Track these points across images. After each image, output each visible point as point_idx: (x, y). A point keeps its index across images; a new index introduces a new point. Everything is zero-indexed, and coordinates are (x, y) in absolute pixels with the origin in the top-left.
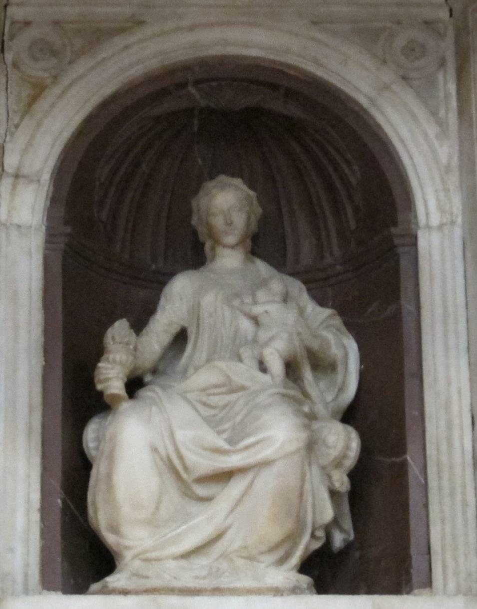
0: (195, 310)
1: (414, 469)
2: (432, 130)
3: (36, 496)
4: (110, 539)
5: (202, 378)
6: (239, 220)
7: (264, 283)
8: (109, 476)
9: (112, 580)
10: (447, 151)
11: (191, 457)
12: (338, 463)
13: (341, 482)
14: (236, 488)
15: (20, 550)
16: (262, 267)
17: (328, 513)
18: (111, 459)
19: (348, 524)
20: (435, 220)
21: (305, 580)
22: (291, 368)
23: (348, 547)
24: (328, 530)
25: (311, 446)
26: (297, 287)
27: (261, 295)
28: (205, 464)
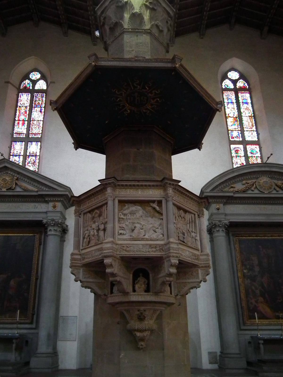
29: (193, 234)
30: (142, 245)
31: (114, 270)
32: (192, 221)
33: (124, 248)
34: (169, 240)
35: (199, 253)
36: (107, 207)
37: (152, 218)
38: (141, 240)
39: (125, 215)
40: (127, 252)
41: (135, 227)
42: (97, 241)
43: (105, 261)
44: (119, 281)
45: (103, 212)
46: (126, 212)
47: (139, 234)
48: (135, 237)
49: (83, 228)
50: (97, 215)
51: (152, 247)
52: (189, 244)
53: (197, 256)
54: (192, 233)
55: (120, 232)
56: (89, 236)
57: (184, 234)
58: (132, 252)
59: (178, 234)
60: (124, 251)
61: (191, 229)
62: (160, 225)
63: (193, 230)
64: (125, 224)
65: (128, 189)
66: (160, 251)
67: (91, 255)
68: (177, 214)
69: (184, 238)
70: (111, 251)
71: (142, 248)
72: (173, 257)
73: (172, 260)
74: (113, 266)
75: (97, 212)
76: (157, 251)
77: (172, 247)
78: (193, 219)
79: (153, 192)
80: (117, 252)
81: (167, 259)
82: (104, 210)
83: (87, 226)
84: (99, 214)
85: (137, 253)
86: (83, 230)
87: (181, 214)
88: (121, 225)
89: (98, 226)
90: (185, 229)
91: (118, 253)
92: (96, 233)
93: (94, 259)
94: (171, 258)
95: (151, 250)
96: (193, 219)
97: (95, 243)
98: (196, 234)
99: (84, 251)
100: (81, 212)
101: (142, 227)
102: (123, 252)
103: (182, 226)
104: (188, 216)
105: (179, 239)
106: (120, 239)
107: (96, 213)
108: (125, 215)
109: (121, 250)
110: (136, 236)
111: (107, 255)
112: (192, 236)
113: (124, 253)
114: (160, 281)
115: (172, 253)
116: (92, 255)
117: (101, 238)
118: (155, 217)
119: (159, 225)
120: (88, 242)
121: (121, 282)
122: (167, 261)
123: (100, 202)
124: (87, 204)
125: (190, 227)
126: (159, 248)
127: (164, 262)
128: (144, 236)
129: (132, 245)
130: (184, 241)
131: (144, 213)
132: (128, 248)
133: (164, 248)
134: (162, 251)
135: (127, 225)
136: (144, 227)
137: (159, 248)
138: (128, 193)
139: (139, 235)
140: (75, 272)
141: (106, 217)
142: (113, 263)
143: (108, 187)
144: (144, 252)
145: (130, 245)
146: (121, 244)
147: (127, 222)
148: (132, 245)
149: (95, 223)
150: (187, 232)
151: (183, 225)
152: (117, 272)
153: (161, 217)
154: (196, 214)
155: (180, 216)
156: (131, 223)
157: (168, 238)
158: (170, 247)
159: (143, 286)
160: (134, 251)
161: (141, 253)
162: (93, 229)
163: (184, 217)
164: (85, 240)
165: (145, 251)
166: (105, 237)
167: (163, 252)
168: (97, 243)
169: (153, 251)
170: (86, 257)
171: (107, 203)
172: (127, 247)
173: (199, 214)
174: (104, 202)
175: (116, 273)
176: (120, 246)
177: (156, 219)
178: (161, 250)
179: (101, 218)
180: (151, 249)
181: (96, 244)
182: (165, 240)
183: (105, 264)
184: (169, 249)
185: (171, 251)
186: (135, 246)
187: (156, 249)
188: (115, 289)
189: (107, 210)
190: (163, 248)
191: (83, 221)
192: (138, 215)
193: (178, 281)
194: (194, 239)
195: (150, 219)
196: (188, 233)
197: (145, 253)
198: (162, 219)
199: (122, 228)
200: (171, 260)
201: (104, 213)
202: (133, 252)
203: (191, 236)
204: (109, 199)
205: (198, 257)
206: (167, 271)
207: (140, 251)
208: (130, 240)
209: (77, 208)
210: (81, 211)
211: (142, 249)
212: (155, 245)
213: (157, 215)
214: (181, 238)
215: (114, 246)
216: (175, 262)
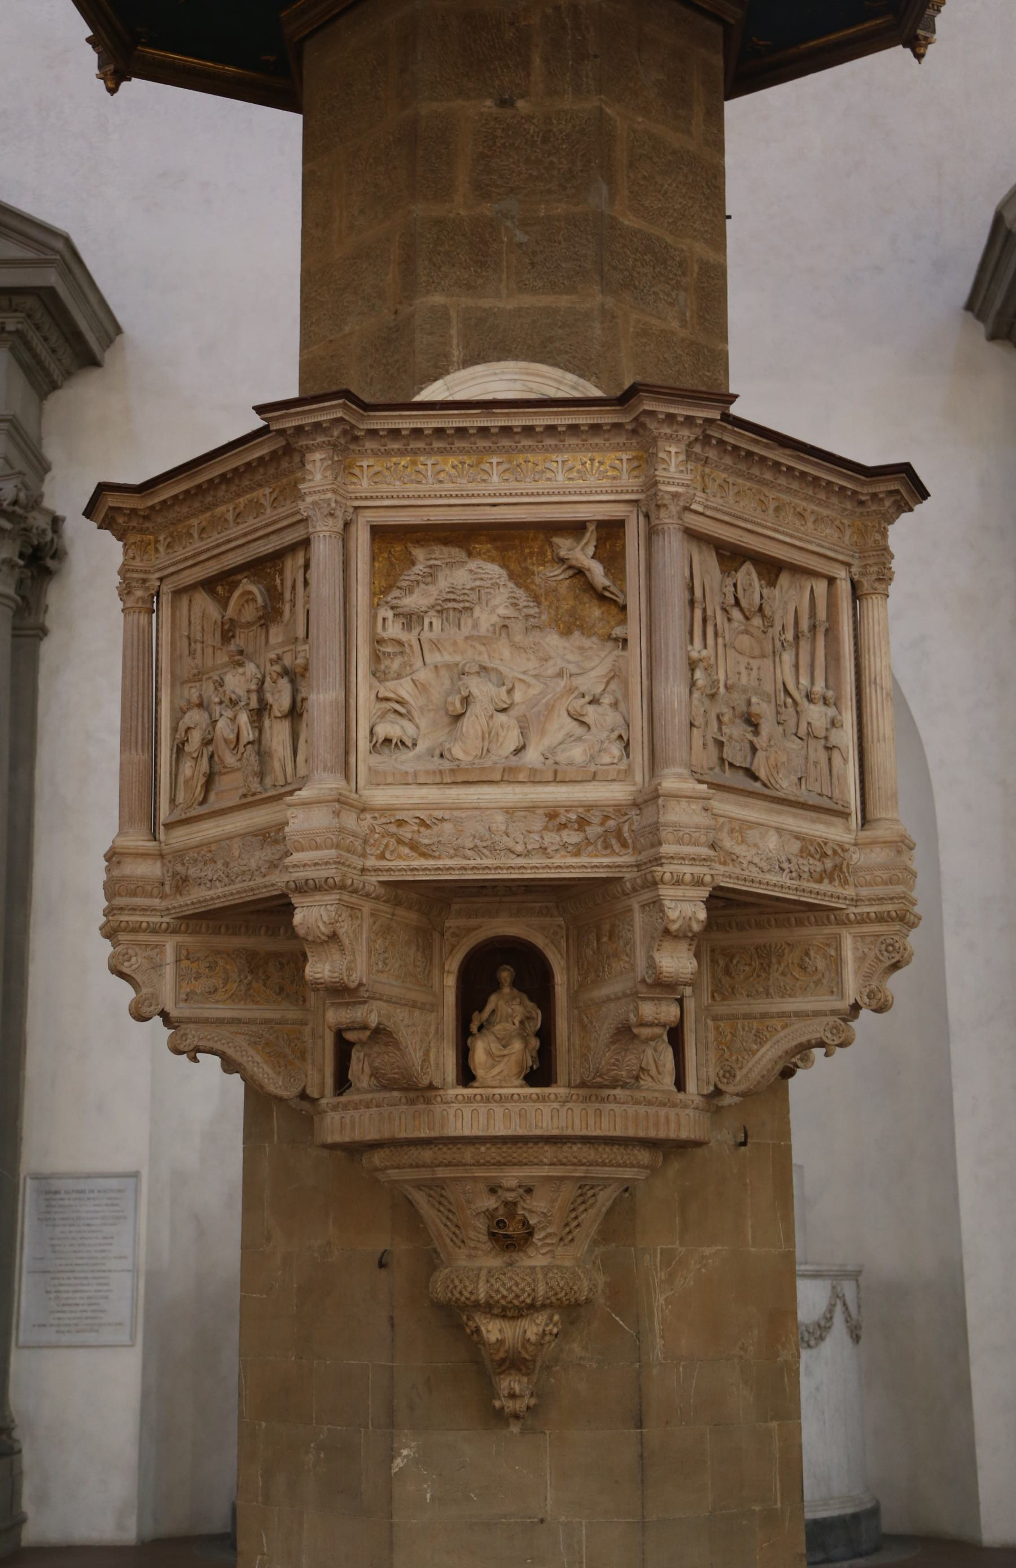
0: (497, 1006)
1: (553, 1051)
2: (559, 957)
3: (455, 1061)
4: (474, 1072)
5: (498, 1028)
6: (509, 980)
7: (514, 998)
8: (473, 1055)
9: (475, 1084)
10: (563, 963)
11: (494, 1051)
12: (534, 1049)
13: (535, 1054)
14: (506, 1059)
15: (451, 1074)
16: (515, 991)
17: (530, 1063)
18: (474, 1052)
19: (538, 1063)
20: (560, 983)
21: (524, 1082)
22: (522, 1022)
23: (538, 1068)
24: (532, 1067)
25: (526, 1046)
26: (525, 997)
27: (514, 1003)
28: (497, 1053)
29: (816, 714)
30: (509, 811)
31: (349, 969)
32: (813, 628)
33: (406, 833)
34: (656, 781)
35: (849, 830)
36: (307, 566)
37: (566, 632)
38: (498, 777)
39: (410, 619)
40: (423, 855)
41: (466, 701)
42: (257, 780)
43: (298, 918)
44: (379, 1024)
45: (287, 596)
46: (412, 602)
47: (490, 742)
48: (462, 766)
49: (173, 686)
50: (249, 614)
51: (563, 820)
52: (786, 785)
53: (835, 852)
54: (812, 706)
55: (383, 731)
56: (207, 742)
57: (752, 722)
58: (452, 858)
59: (720, 729)
60: (406, 850)
61: (804, 681)
62: (614, 675)
63: (819, 687)
64: (413, 680)
65: (430, 452)
66: (607, 846)
67: (220, 864)
68: (718, 599)
69: (754, 750)
70: (332, 853)
71: (503, 828)
72: (678, 882)
73: (673, 905)
74: (346, 941)
75: (250, 593)
76: (590, 848)
77: (674, 825)
78: (822, 614)
79: (571, 469)
80: (364, 855)
81: (646, 896)
82: (294, 587)
83: (198, 677)
84: (265, 607)
85: (478, 862)
86: (172, 702)
87: (740, 595)
89: (260, 690)
90: (769, 688)
91: (371, 862)
92: (248, 734)
93: (239, 892)
94: (661, 892)
95: (558, 838)
96: (822, 614)
97: (245, 796)
98: (831, 711)
99: (181, 838)
100: (158, 583)
101: (504, 696)
102: (399, 857)
103: (749, 668)
105: (722, 760)
106: (378, 779)
107: (248, 597)
108: (410, 619)
109: (387, 846)
110: (470, 758)
111: (311, 882)
112: (809, 723)
113: (402, 864)
114: (605, 1031)
115: (672, 858)
116: (226, 864)
117: (277, 765)
118: (586, 630)
119: (605, 680)
120: (202, 780)
121: (390, 1034)
122: (643, 906)
123: (268, 535)
124: (196, 535)
125: (797, 666)
126: (602, 824)
127: (630, 910)
128: (518, 751)
129: (447, 815)
130: (753, 769)
131: (522, 603)
132: (429, 831)
133: (627, 824)
134: (616, 847)
135: (422, 684)
136: (518, 696)
137: (600, 830)
138: (428, 485)
139: (488, 751)
140: (134, 967)
141: (301, 632)
142: (344, 929)
143: (310, 449)
144: (513, 852)
145: (439, 814)
146: (384, 810)
147: (425, 664)
149: (241, 664)
150: (777, 705)
151: (755, 663)
152: (364, 981)
153: (618, 631)
154: (841, 573)
155: (737, 603)
156: (443, 672)
157: (654, 762)
158: (658, 823)
159: (517, 1046)
160: (457, 851)
161: (496, 862)
162: (233, 703)
163: (761, 605)
164: (187, 768)
165: (519, 848)
166: (301, 757)
167: (624, 851)
168: (254, 794)
169: (565, 846)
170: (193, 872)
171: (306, 543)
172: (422, 823)
173: (856, 578)
174: (290, 537)
175: (361, 984)
176: (384, 820)
177: (587, 642)
178: (614, 841)
179: (273, 630)
180: (553, 835)
181: (250, 799)
182: (638, 778)
183: (301, 932)
184: (653, 835)
185: (666, 849)
186: (463, 814)
187: (582, 835)
188: (359, 1068)
189: (306, 583)
190: (625, 822)
191: (173, 644)
192: (485, 619)
193: (721, 1009)
194: (823, 742)
195: (553, 640)
196: (786, 707)
198: (625, 641)
200: (667, 903)
201: (293, 602)
202: (452, 852)
203: (803, 730)
204: (318, 529)
205: (838, 860)
206: (641, 963)
207: (493, 849)
208: (438, 780)
209: (134, 558)
210: (158, 575)
211: (507, 835)
212: (580, 810)
213: (595, 612)
214: (736, 754)
215: (350, 820)
216: (689, 914)
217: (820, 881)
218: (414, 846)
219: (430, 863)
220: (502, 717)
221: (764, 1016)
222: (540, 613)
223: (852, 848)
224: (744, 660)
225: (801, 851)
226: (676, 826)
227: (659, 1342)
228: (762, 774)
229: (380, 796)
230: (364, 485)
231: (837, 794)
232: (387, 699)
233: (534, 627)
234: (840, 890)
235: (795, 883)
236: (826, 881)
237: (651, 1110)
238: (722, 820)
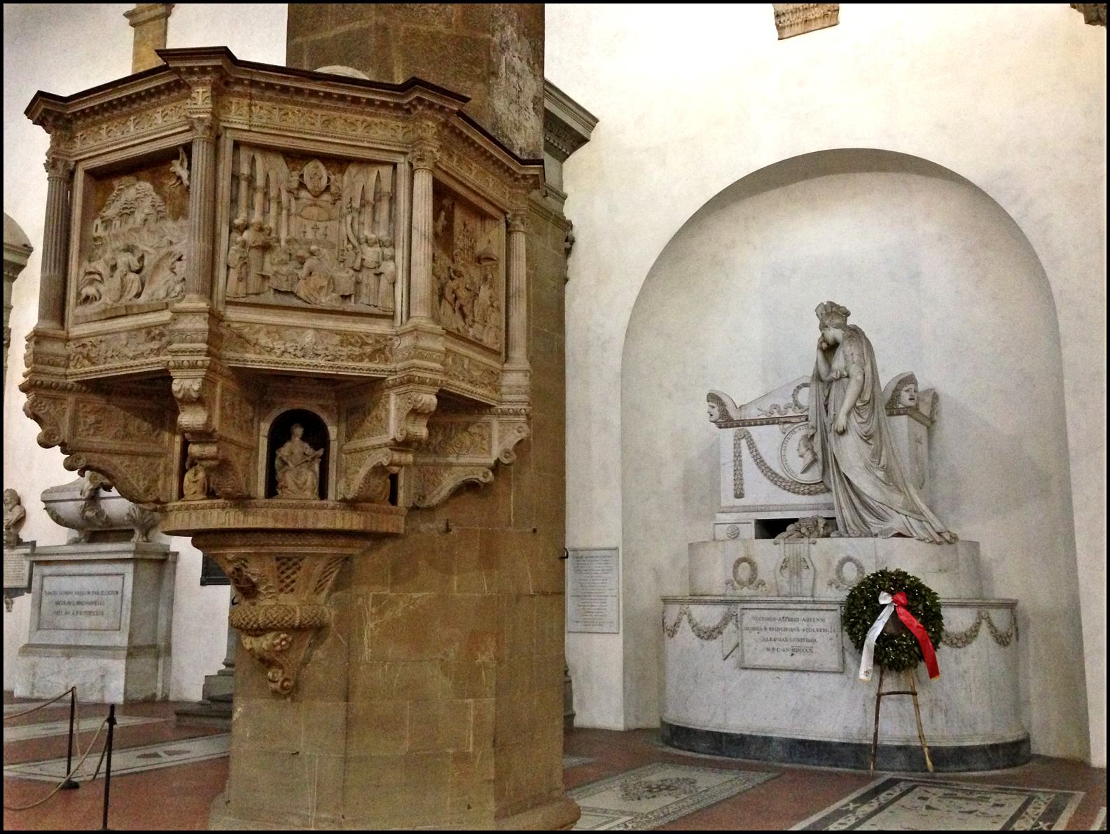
29: (371, 254)
54: (369, 249)
55: (90, 290)
60: (86, 362)
80: (68, 367)
88: (88, 266)
102: (83, 366)
103: (316, 228)
104: (356, 182)
145: (100, 338)
148: (103, 338)
151: (321, 225)
197: (131, 362)
199: (93, 277)
203: (357, 265)
212: (161, 328)
217: (362, 360)
218: (88, 357)
219: (93, 368)
220: (132, 276)
221: (362, 450)
222: (166, 209)
223: (395, 338)
224: (312, 224)
225: (342, 342)
226: (182, 332)
227: (367, 652)
228: (302, 294)
229: (75, 331)
230: (78, 146)
231: (380, 304)
232: (91, 273)
233: (161, 218)
234: (382, 366)
235: (331, 363)
236: (367, 360)
237: (289, 511)
238: (257, 327)
